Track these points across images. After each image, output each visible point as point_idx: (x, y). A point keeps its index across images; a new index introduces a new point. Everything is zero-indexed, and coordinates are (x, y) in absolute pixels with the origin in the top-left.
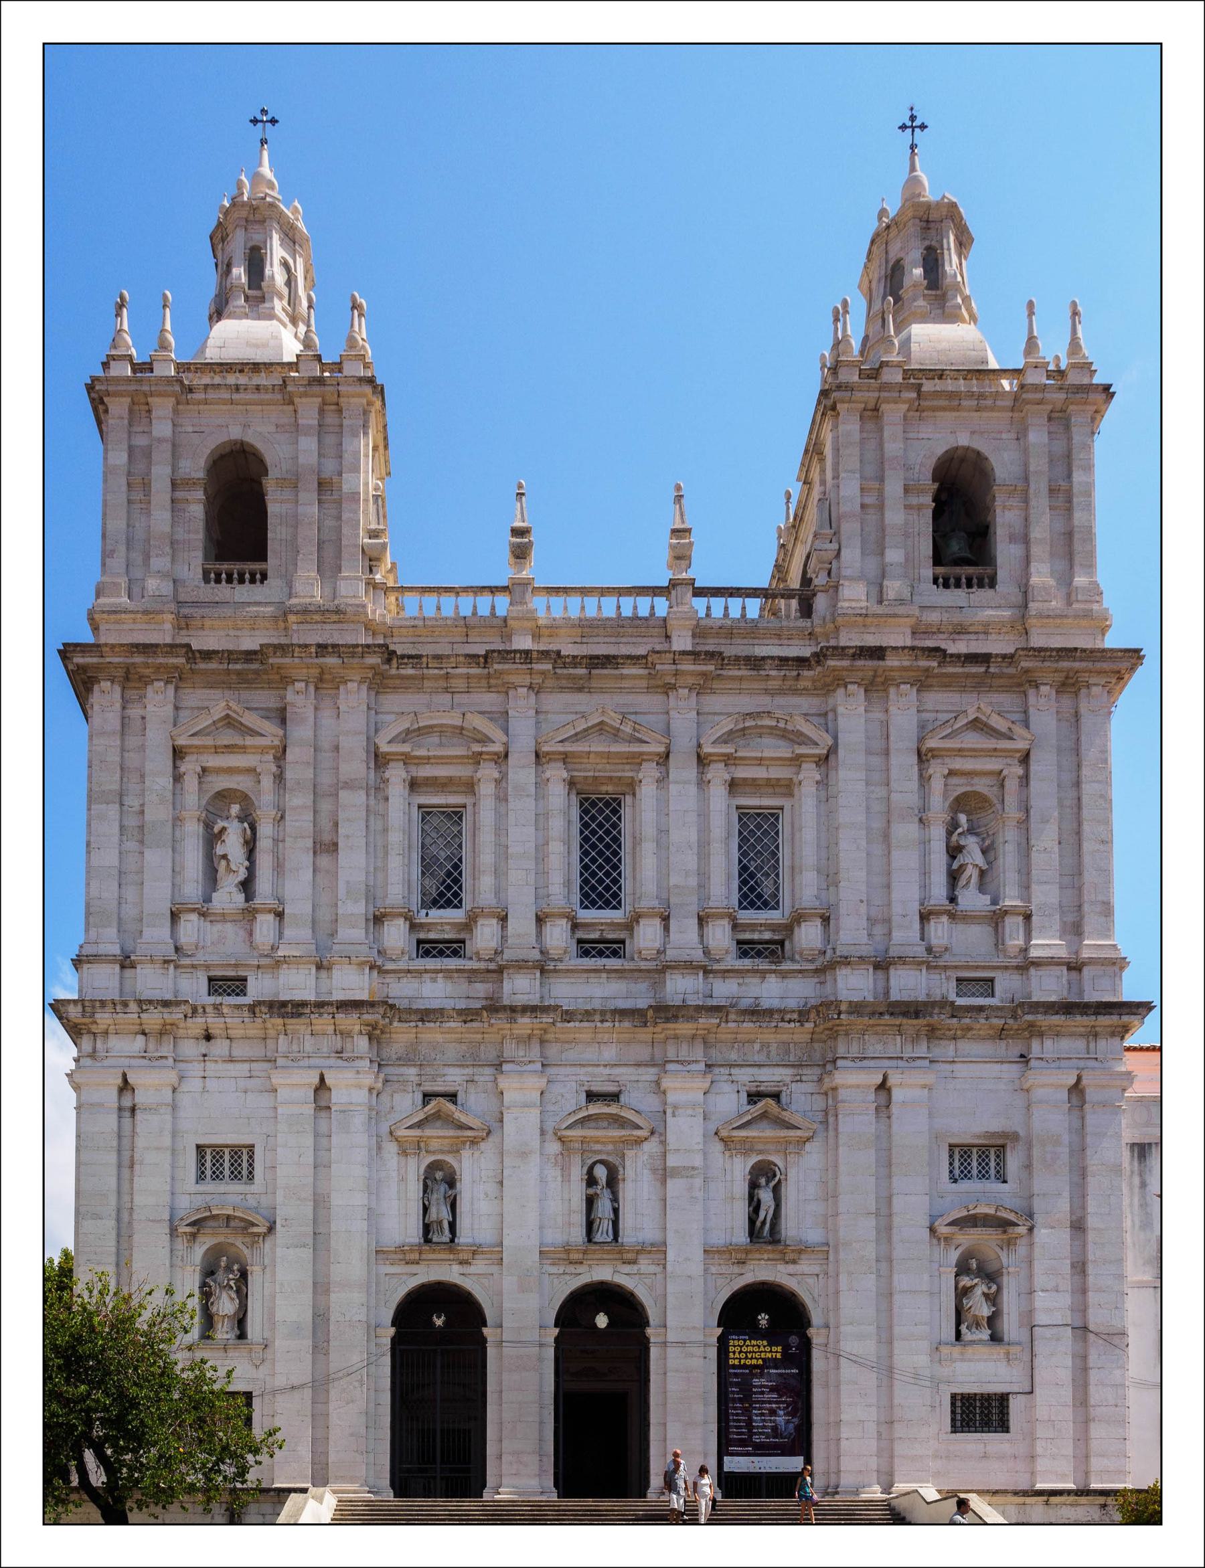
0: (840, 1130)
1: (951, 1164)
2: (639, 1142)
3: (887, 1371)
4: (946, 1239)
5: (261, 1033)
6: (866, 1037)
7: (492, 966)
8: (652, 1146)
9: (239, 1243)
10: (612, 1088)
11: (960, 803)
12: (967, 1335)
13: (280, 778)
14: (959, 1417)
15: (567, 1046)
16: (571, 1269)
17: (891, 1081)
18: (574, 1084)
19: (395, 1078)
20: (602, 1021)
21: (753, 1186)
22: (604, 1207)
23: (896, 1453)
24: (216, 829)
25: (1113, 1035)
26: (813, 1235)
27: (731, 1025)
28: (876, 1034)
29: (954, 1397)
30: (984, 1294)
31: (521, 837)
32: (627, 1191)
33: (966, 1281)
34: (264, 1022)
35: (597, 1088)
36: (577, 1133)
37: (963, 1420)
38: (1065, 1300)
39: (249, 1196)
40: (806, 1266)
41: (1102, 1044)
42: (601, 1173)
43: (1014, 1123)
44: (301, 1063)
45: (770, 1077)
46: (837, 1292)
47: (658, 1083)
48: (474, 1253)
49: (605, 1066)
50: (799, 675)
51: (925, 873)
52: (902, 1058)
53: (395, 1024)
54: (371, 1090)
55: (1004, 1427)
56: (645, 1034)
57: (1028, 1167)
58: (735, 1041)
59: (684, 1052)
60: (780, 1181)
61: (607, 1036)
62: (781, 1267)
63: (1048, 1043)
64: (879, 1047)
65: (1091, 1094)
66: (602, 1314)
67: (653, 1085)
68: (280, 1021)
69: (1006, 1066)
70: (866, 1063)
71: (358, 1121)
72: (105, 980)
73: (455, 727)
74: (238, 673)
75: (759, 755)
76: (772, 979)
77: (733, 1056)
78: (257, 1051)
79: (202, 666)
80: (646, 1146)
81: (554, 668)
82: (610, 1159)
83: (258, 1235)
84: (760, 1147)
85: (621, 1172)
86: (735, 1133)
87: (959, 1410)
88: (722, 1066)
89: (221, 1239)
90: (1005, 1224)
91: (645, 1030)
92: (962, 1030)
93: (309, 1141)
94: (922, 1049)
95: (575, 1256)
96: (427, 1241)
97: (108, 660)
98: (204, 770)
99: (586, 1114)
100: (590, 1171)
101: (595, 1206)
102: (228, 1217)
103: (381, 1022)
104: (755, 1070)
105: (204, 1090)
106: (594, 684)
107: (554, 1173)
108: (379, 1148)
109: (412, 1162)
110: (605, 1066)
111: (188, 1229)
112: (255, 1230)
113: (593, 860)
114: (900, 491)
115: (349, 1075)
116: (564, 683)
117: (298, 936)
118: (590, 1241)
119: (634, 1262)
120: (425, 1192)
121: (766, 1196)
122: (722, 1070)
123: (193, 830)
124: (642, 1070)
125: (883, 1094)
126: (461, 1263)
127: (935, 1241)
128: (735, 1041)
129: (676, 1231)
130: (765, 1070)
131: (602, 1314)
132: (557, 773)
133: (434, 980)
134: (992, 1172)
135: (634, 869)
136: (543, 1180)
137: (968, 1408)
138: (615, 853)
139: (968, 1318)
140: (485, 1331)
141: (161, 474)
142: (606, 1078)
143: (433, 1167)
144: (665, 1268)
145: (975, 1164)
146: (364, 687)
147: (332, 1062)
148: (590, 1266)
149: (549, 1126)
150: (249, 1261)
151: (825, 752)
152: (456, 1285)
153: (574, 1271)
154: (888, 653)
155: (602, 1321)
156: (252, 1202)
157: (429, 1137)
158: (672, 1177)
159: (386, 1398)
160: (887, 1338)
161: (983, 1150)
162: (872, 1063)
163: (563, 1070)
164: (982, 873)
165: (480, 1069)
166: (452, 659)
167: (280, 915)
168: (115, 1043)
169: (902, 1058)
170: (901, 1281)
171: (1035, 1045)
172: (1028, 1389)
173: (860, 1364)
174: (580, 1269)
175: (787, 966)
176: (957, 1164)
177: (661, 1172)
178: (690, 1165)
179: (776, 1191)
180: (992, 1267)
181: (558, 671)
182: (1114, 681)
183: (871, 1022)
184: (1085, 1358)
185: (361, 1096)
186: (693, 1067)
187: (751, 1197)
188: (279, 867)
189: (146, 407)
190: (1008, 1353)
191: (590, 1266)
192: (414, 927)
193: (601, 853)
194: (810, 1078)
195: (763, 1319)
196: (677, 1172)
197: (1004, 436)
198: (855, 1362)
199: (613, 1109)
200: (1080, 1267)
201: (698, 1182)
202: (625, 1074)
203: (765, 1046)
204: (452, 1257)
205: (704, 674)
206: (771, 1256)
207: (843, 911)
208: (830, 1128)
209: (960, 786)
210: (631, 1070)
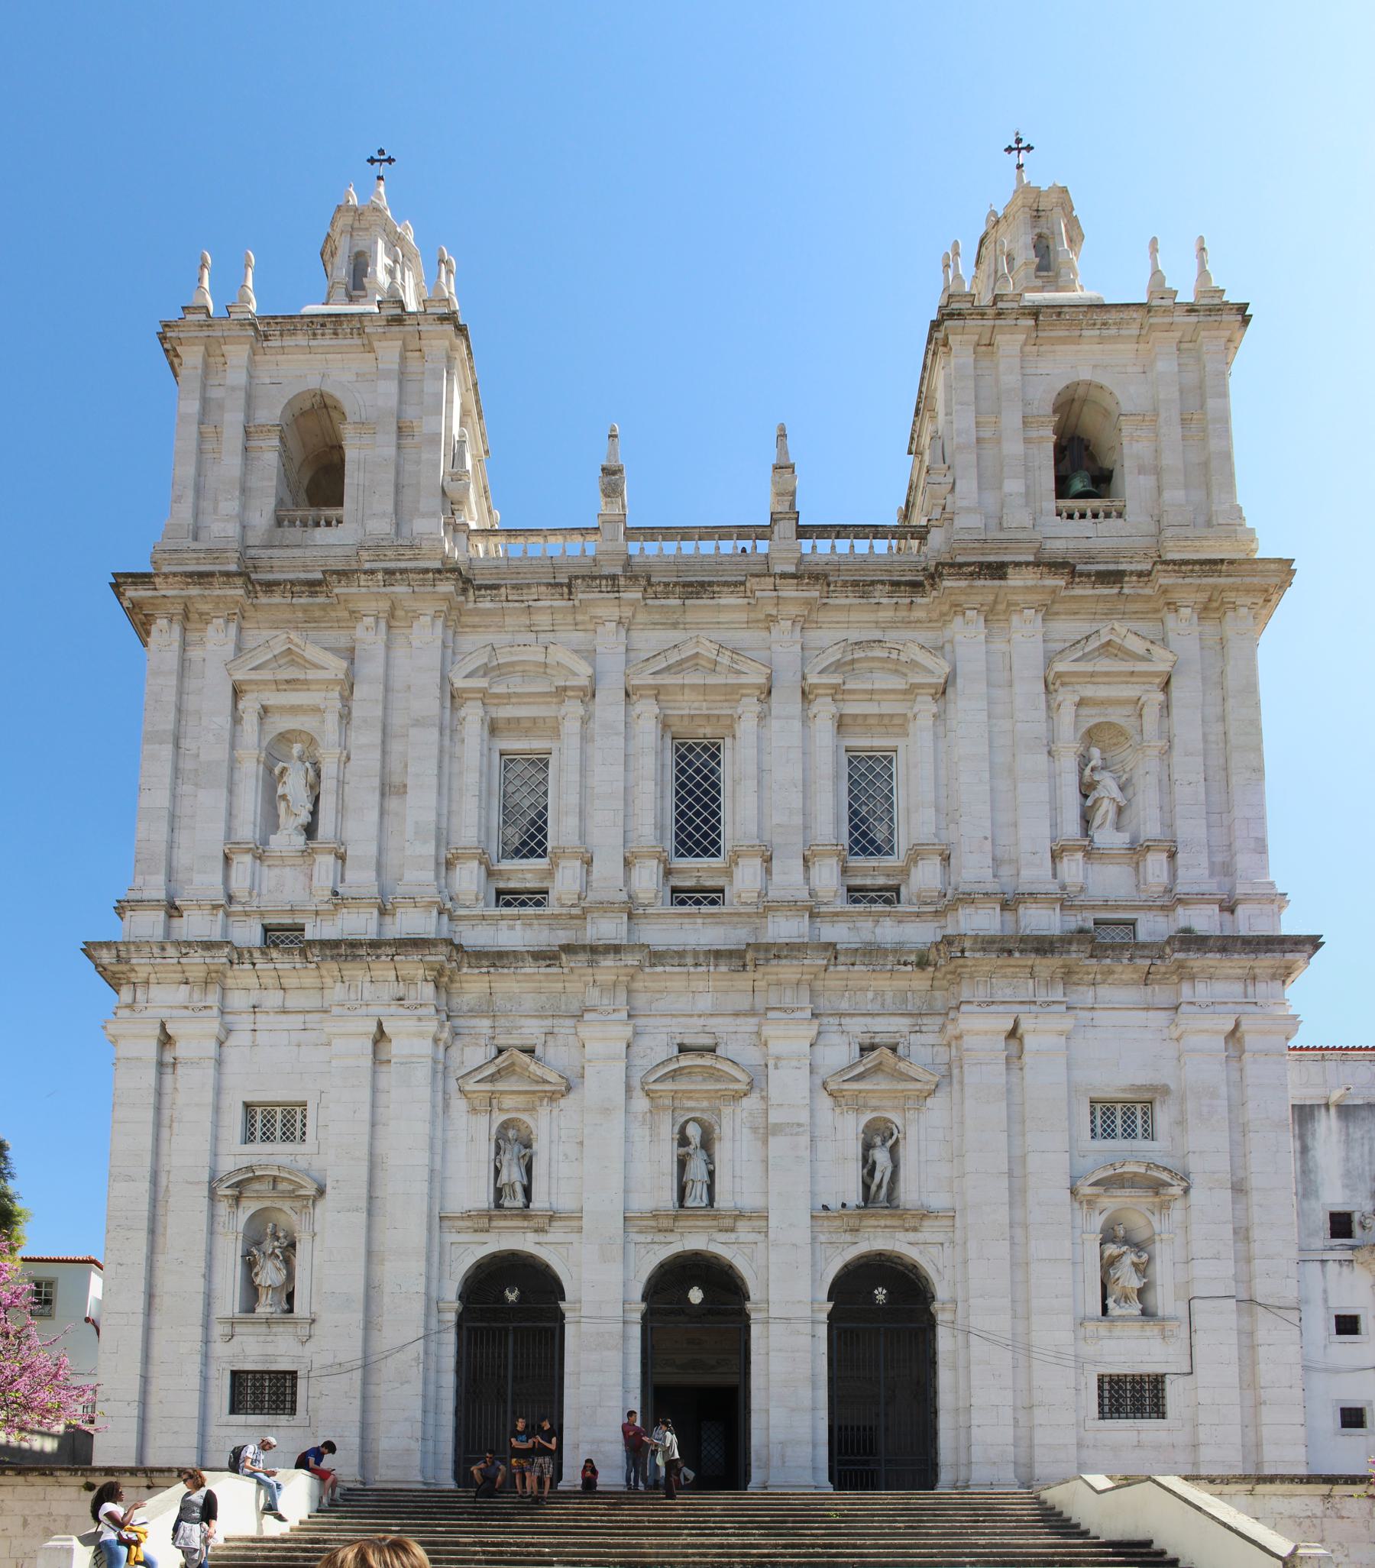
1: (1092, 1122)
2: (737, 1097)
3: (1022, 1348)
4: (1089, 1202)
5: (317, 982)
6: (994, 980)
7: (575, 911)
8: (751, 1102)
9: (286, 1208)
10: (706, 1041)
11: (1091, 736)
12: (1114, 1309)
13: (345, 717)
14: (1106, 1401)
15: (658, 996)
16: (660, 1237)
17: (1025, 1025)
18: (664, 1036)
19: (466, 1031)
20: (696, 965)
21: (868, 1147)
22: (697, 1169)
23: (1036, 1442)
24: (277, 771)
25: (1273, 977)
26: (937, 1201)
27: (841, 968)
28: (1005, 976)
29: (1101, 1379)
30: (1134, 1264)
31: (607, 776)
32: (722, 1152)
34: (318, 968)
35: (688, 1041)
36: (668, 1086)
38: (1228, 1268)
39: (298, 1158)
40: (929, 1232)
41: (1261, 987)
42: (694, 1132)
43: (1164, 1076)
44: (359, 1012)
45: (888, 1026)
46: (966, 1262)
47: (758, 1034)
48: (551, 1218)
50: (912, 602)
51: (1055, 809)
52: (1035, 1002)
53: (465, 970)
54: (436, 1040)
55: (1158, 1411)
56: (744, 981)
57: (1181, 1122)
58: (846, 988)
59: (788, 1000)
60: (897, 1140)
61: (702, 983)
62: (901, 1235)
63: (1200, 987)
64: (1009, 991)
65: (1251, 1041)
66: (696, 1288)
67: (753, 1036)
68: (334, 966)
69: (1151, 1014)
70: (993, 1008)
71: (422, 1073)
72: (148, 924)
73: (537, 664)
74: (305, 609)
75: (870, 687)
76: (888, 922)
77: (844, 1005)
78: (312, 1001)
79: (263, 600)
80: (745, 1102)
81: (644, 599)
82: (705, 1117)
83: (306, 1197)
84: (874, 1102)
85: (717, 1131)
86: (846, 1086)
87: (1106, 1394)
88: (831, 1015)
89: (267, 1203)
90: (1157, 1187)
91: (744, 975)
92: (1102, 973)
93: (366, 1095)
94: (1057, 994)
95: (665, 1223)
96: (499, 1206)
97: (163, 593)
98: (265, 710)
99: (676, 1066)
100: (682, 1131)
101: (687, 1168)
102: (275, 1179)
103: (447, 966)
104: (868, 1020)
105: (254, 1044)
106: (689, 617)
107: (640, 1133)
108: (446, 1106)
109: (483, 1120)
110: (700, 1016)
111: (229, 1192)
112: (302, 1192)
114: (1018, 422)
115: (411, 1024)
116: (657, 617)
117: (361, 879)
118: (681, 1206)
119: (732, 1230)
120: (497, 1153)
121: (881, 1156)
122: (831, 1020)
123: (250, 770)
124: (741, 1020)
125: (1014, 1043)
126: (536, 1231)
127: (1076, 1205)
128: (846, 988)
130: (879, 1019)
132: (647, 710)
133: (511, 928)
134: (1139, 1130)
136: (627, 1139)
137: (1117, 1392)
138: (714, 799)
139: (1115, 1291)
140: (563, 1305)
141: (233, 420)
142: (700, 1029)
143: (505, 1126)
144: (767, 1236)
145: (1119, 1122)
146: (440, 622)
147: (393, 1009)
148: (682, 1234)
150: (297, 1228)
151: (942, 681)
152: (532, 1256)
153: (663, 1240)
154: (1010, 570)
155: (696, 1296)
156: (302, 1163)
157: (502, 1092)
158: (774, 1135)
159: (449, 1380)
160: (1021, 1310)
161: (1129, 1106)
162: (1001, 1008)
163: (651, 1021)
164: (1120, 811)
165: (561, 1021)
166: (534, 590)
167: (342, 858)
168: (155, 991)
169: (1035, 1002)
171: (1186, 989)
172: (1189, 1371)
174: (670, 1237)
175: (900, 908)
176: (1098, 1122)
177: (761, 1131)
178: (795, 1121)
179: (893, 1151)
180: (1141, 1235)
181: (649, 602)
182: (1261, 601)
183: (1000, 962)
184: (1251, 1334)
185: (425, 1047)
186: (798, 1015)
187: (865, 1159)
188: (341, 810)
189: (222, 359)
190: (1163, 1330)
191: (682, 1234)
192: (490, 874)
194: (931, 1028)
197: (1129, 369)
198: (987, 1339)
199: (707, 1061)
200: (1242, 1233)
201: (805, 1140)
202: (720, 1024)
203: (879, 994)
204: (526, 1224)
205: (807, 602)
206: (889, 1223)
208: (955, 1080)
209: (1092, 717)
210: (729, 1020)
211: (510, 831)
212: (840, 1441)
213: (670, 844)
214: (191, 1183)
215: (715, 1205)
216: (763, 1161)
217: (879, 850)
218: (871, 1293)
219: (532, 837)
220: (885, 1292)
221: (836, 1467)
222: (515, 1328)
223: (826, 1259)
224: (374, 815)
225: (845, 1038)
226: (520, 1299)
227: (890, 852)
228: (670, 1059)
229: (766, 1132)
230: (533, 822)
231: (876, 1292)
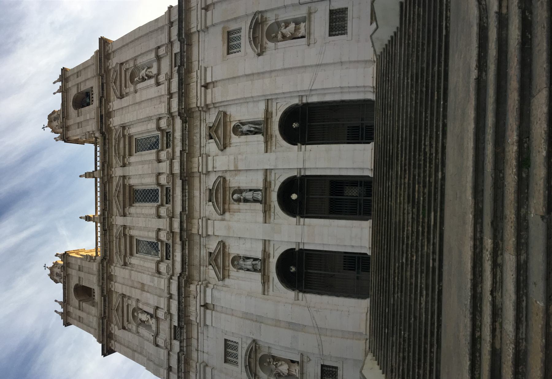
0: (220, 101)
22: (249, 195)
33: (280, 36)
37: (342, 30)
42: (235, 196)
49: (200, 195)
60: (240, 123)
62: (274, 119)
67: (206, 176)
82: (231, 193)
99: (215, 203)
104: (202, 137)
105: (207, 353)
107: (237, 216)
113: (148, 198)
121: (245, 128)
122: (202, 150)
129: (258, 165)
130: (202, 134)
135: (149, 185)
142: (204, 195)
149: (220, 217)
158: (238, 168)
170: (279, 66)
177: (236, 172)
179: (243, 124)
187: (246, 134)
193: (146, 196)
196: (236, 165)
207: (157, 113)
211: (152, 253)
212: (353, 140)
213: (155, 204)
215: (261, 189)
216: (247, 171)
217: (158, 140)
218: (294, 129)
219: (154, 246)
221: (364, 141)
223: (281, 147)
224: (148, 294)
225: (207, 145)
227: (158, 136)
228: (213, 205)
229: (237, 171)
230: (150, 246)
231: (294, 127)
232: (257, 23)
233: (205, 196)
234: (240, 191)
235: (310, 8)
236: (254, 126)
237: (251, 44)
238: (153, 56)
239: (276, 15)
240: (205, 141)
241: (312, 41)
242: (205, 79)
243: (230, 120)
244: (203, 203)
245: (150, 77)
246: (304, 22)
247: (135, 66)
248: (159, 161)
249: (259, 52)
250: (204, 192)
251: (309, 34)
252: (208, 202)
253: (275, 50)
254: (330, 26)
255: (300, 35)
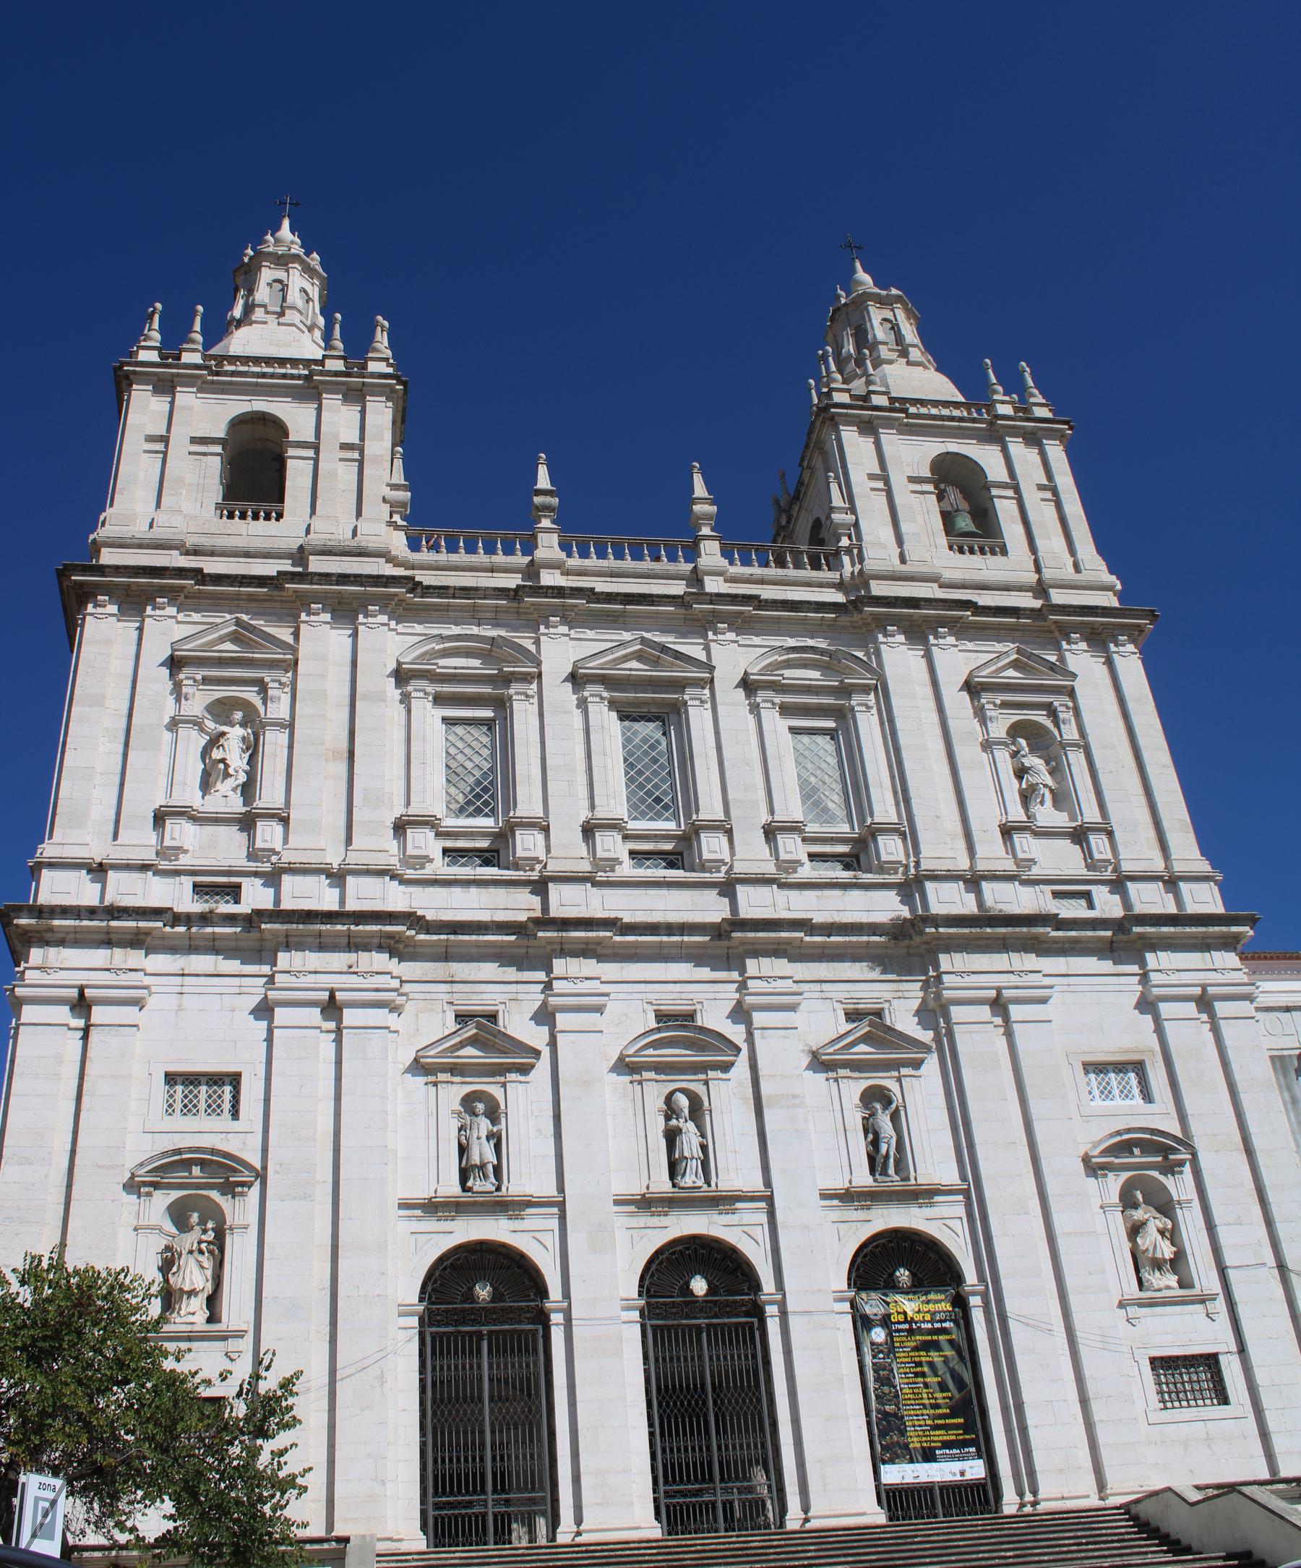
22: (690, 1142)
42: (683, 1101)
60: (897, 1107)
82: (692, 1086)
100: (669, 1099)
122: (811, 985)
131: (698, 1277)
155: (699, 1286)
173: (1034, 1327)
174: (664, 1221)
179: (895, 1117)
187: (866, 1132)
195: (903, 1275)
198: (1027, 1324)
214: (102, 1167)
218: (892, 1275)
220: (907, 1273)
222: (490, 1333)
226: (496, 1296)
232: (1165, 1150)
233: (674, 999)
234: (697, 1111)
235: (1213, 1298)
236: (892, 1154)
237: (1112, 1135)
238: (1091, 814)
239: (1189, 1202)
240: (841, 996)
241: (1133, 1311)
242: (1019, 1001)
243: (904, 1076)
244: (655, 993)
245: (1026, 797)
246: (1182, 1285)
247: (1063, 746)
248: (770, 833)
249: (1094, 1160)
250: (685, 996)
251: (1151, 1304)
252: (656, 1007)
253: (1102, 1207)
254: (1178, 1357)
255: (1146, 1275)
